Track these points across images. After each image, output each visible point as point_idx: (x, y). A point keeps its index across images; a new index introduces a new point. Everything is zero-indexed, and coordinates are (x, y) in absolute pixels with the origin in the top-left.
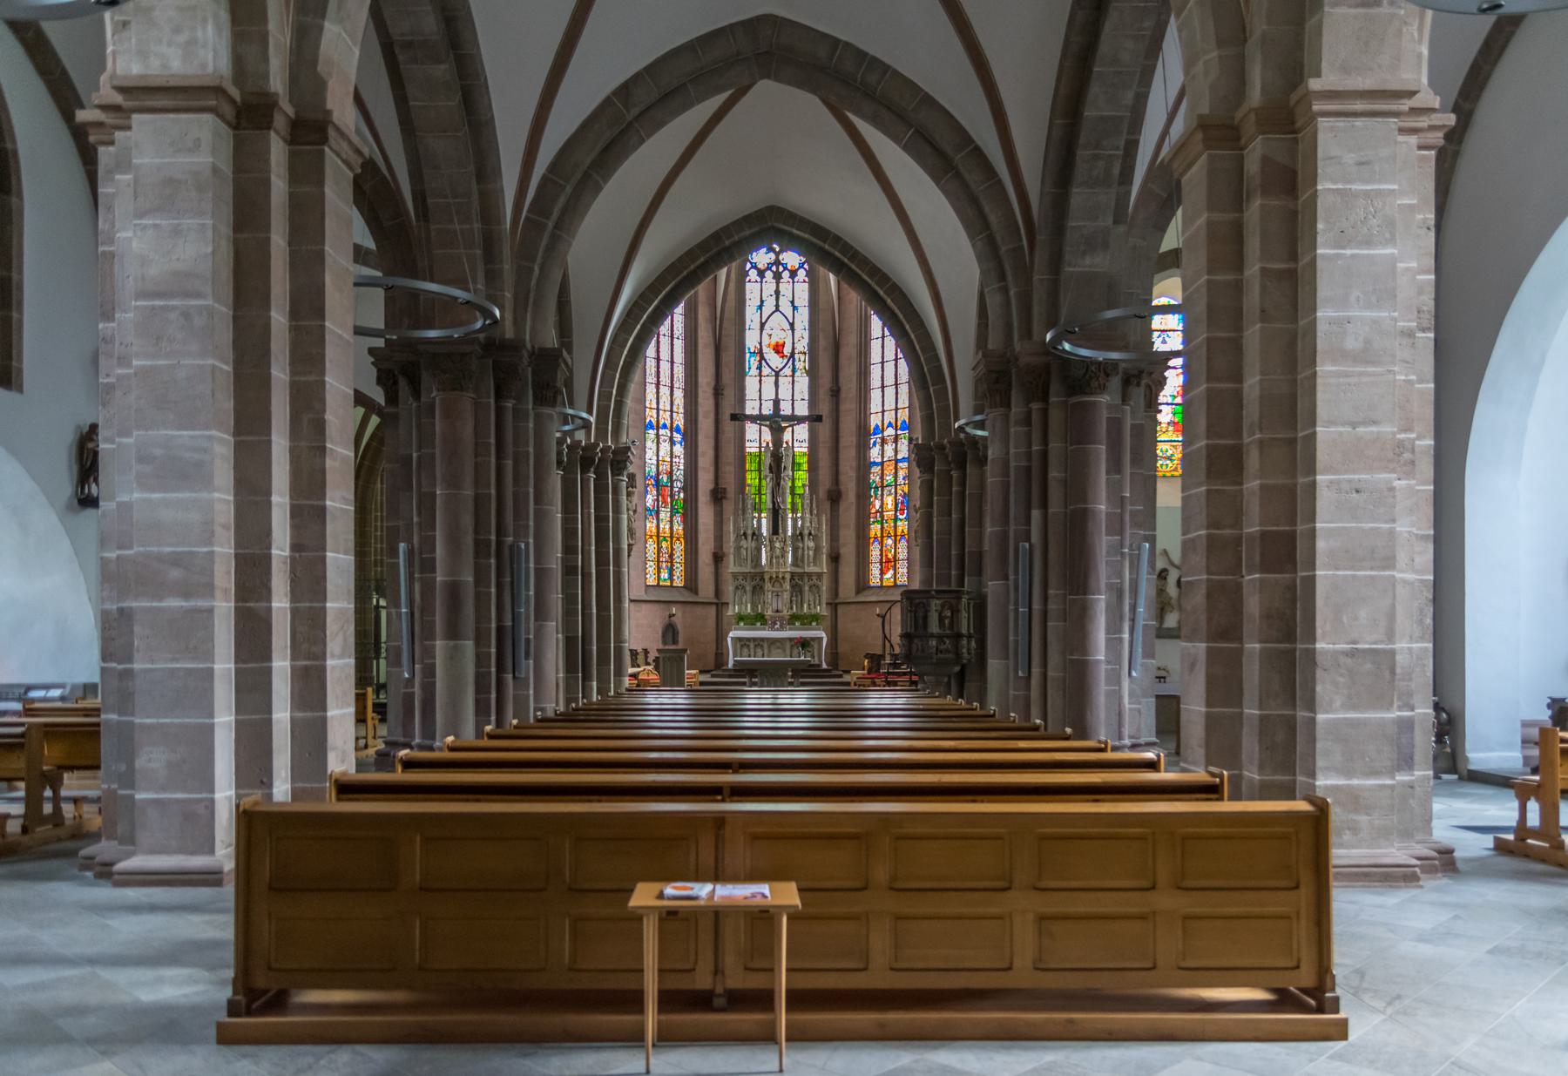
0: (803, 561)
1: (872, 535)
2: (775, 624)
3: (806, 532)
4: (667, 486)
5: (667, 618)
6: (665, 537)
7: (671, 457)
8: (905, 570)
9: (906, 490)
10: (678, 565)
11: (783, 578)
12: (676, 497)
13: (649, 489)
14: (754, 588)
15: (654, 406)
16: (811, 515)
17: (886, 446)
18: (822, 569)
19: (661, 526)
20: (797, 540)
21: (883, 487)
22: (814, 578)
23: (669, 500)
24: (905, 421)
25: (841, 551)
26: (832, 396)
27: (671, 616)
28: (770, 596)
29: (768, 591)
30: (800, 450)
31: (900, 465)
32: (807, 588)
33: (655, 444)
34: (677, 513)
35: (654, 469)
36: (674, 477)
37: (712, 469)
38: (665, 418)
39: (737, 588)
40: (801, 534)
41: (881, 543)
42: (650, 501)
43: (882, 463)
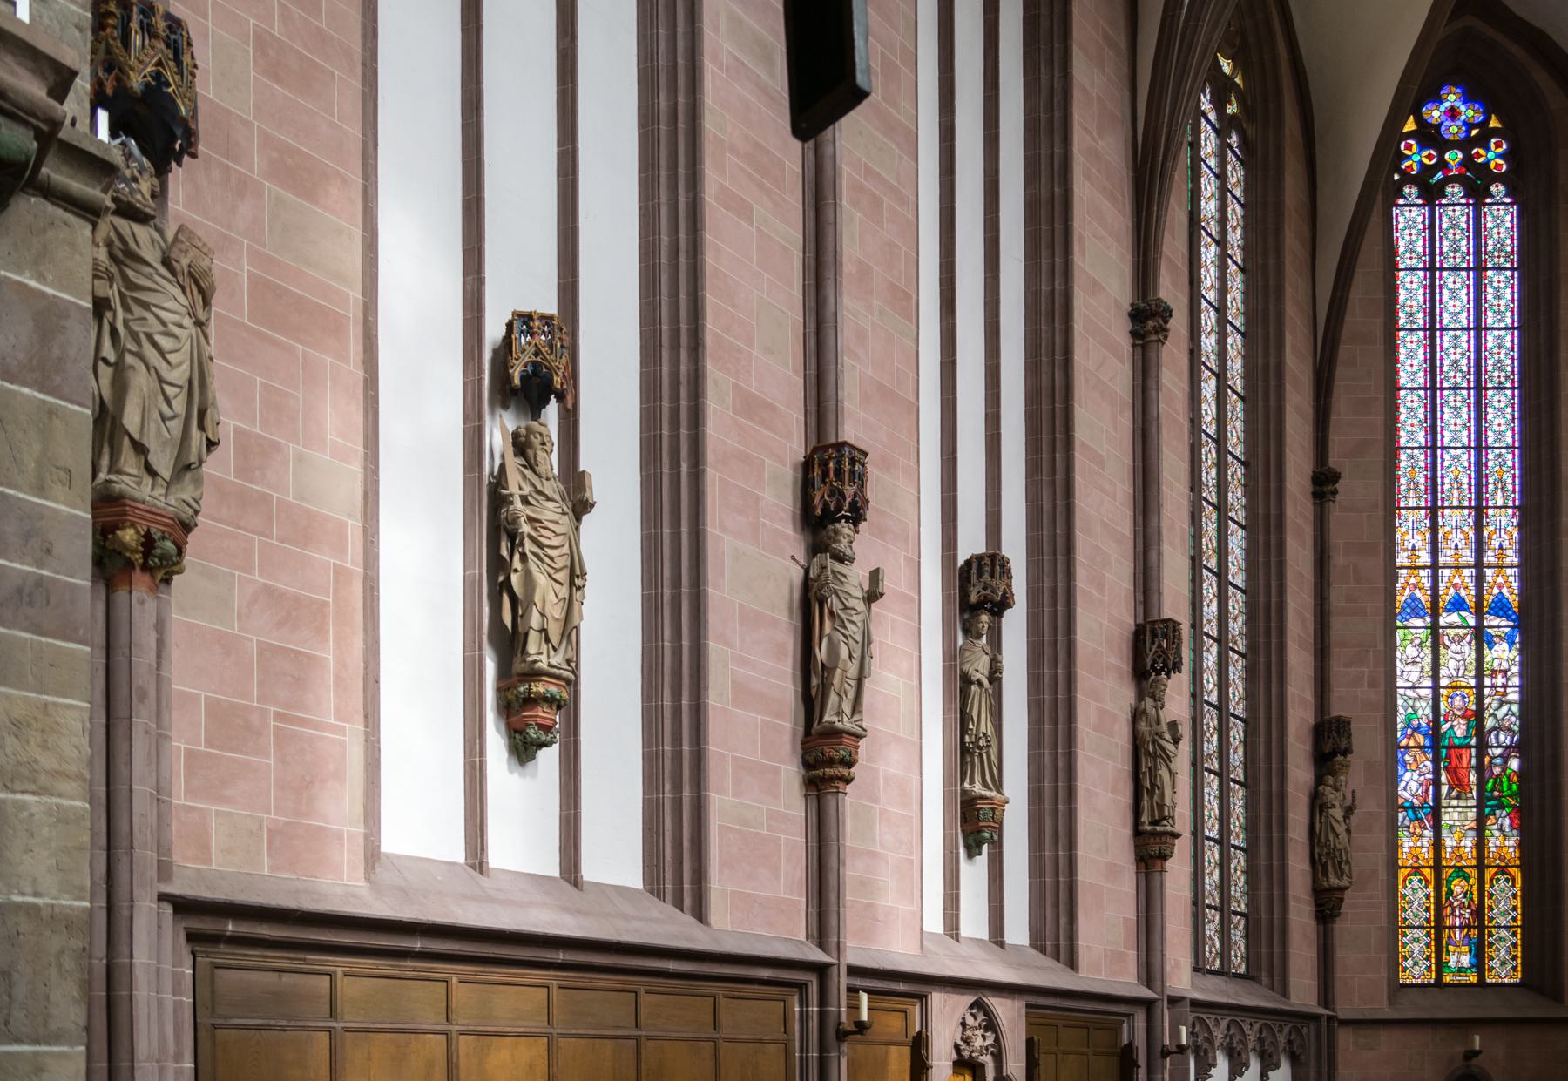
4: (1469, 747)
6: (1461, 868)
7: (1479, 676)
10: (1503, 933)
12: (1497, 770)
19: (1449, 843)
23: (1473, 778)
27: (1471, 1055)
33: (1428, 651)
34: (1502, 807)
35: (1425, 710)
36: (1489, 723)
42: (1414, 785)
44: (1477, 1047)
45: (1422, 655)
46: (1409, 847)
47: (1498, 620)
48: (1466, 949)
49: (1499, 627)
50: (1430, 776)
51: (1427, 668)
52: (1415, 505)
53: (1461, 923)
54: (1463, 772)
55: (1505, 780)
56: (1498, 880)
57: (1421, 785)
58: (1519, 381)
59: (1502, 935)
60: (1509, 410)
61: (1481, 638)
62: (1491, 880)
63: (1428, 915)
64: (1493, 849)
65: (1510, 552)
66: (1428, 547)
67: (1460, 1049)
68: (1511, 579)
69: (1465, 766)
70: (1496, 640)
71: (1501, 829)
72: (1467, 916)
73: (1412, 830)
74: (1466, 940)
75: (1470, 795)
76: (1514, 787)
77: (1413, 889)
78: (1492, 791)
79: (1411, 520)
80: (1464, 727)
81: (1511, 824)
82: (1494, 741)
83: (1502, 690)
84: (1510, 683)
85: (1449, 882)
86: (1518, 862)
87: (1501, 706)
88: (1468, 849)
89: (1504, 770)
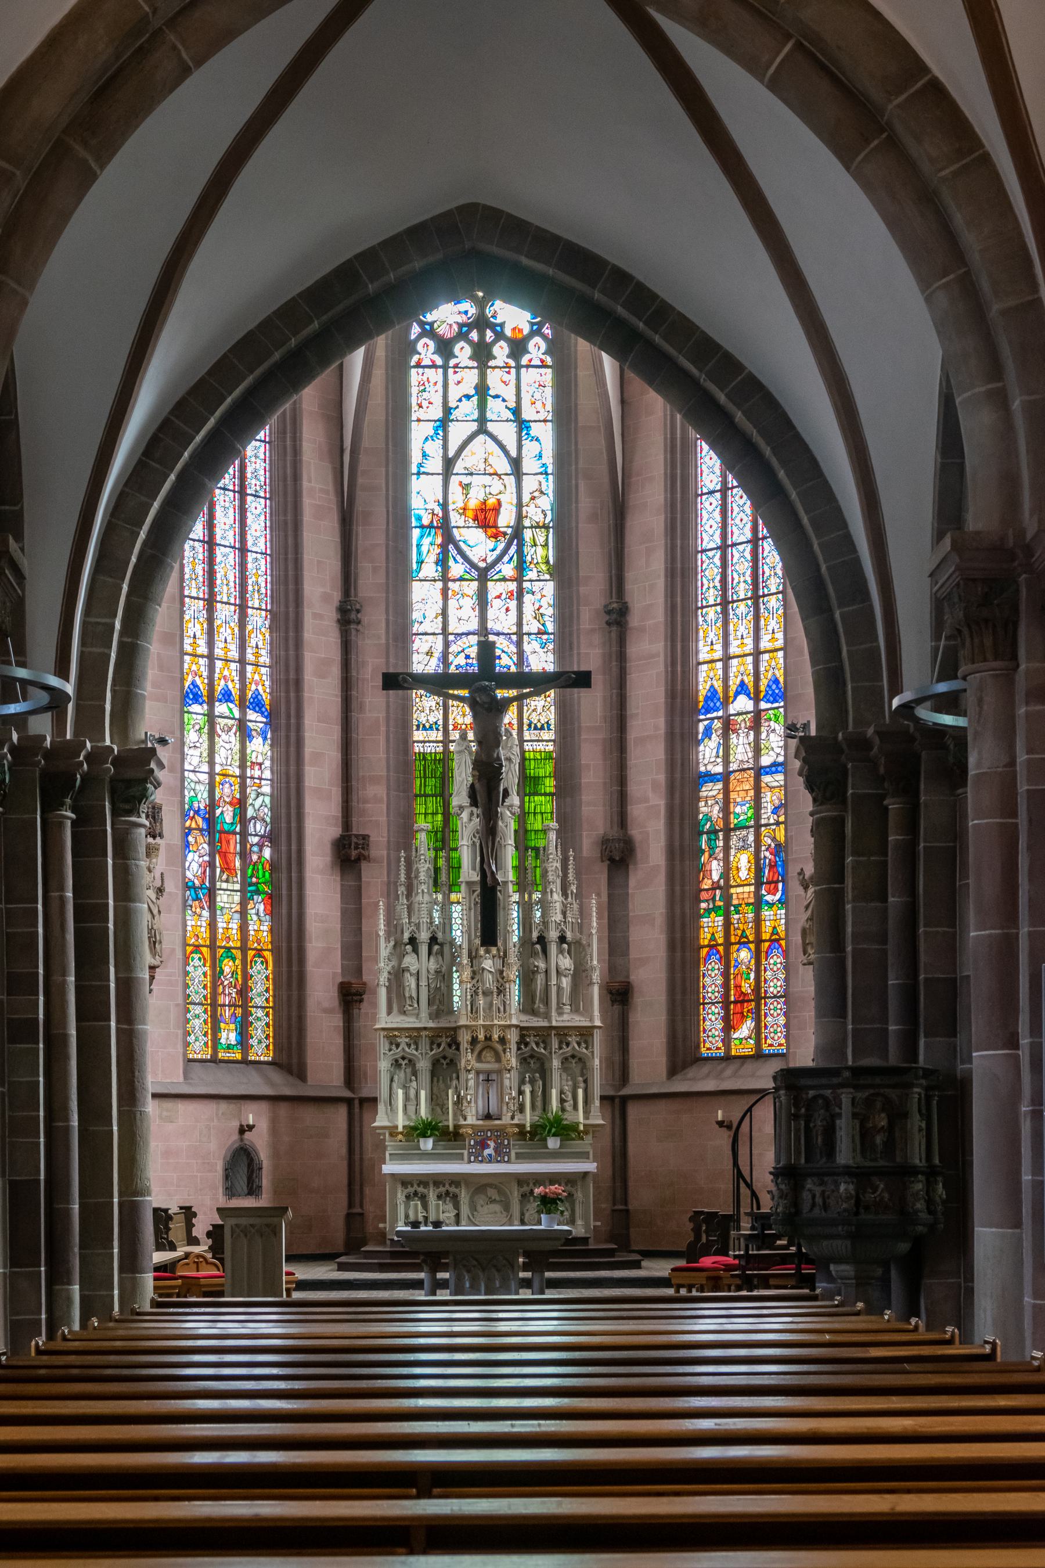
0: (547, 1002)
1: (705, 938)
2: (484, 1145)
3: (553, 935)
4: (234, 833)
5: (236, 1136)
6: (229, 949)
7: (243, 766)
8: (782, 1020)
9: (781, 834)
10: (260, 1013)
11: (502, 1040)
12: (255, 857)
13: (191, 839)
14: (436, 1063)
15: (203, 649)
16: (565, 894)
17: (733, 736)
18: (591, 1020)
19: (221, 925)
20: (534, 954)
21: (728, 831)
22: (573, 1040)
23: (238, 864)
24: (776, 681)
25: (632, 978)
26: (608, 623)
28: (471, 1083)
29: (469, 1071)
30: (541, 746)
31: (766, 779)
32: (556, 1063)
33: (205, 737)
34: (258, 892)
35: (203, 795)
36: (250, 812)
37: (336, 793)
38: (228, 676)
39: (396, 1064)
40: (542, 940)
41: (726, 960)
42: (195, 866)
43: (725, 777)
44: (251, 1123)
45: (201, 741)
46: (192, 926)
47: (256, 715)
48: (232, 1026)
49: (256, 722)
50: (207, 858)
51: (205, 754)
52: (196, 595)
53: (230, 1002)
54: (230, 857)
55: (260, 867)
56: (256, 962)
57: (200, 866)
58: (271, 492)
59: (259, 1015)
60: (263, 518)
61: (244, 732)
62: (251, 962)
63: (205, 992)
64: (252, 933)
65: (263, 652)
66: (205, 637)
67: (236, 1124)
68: (264, 678)
69: (232, 851)
70: (254, 733)
71: (257, 914)
72: (234, 995)
73: (193, 909)
74: (233, 1018)
75: (235, 879)
76: (267, 875)
77: (195, 967)
78: (251, 877)
79: (192, 608)
80: (231, 814)
81: (265, 910)
82: (252, 830)
83: (257, 781)
84: (264, 777)
85: (221, 962)
86: (270, 947)
87: (258, 797)
88: (234, 931)
89: (260, 858)
